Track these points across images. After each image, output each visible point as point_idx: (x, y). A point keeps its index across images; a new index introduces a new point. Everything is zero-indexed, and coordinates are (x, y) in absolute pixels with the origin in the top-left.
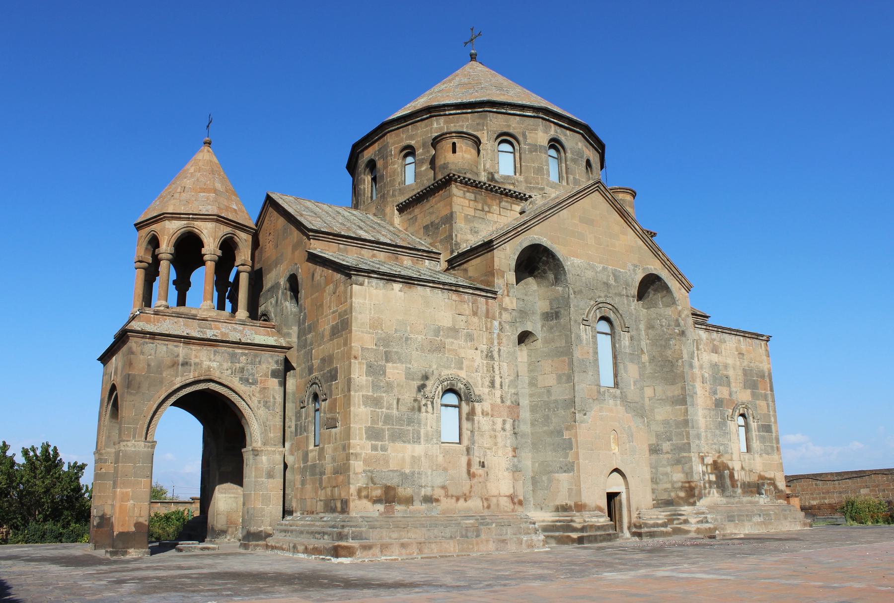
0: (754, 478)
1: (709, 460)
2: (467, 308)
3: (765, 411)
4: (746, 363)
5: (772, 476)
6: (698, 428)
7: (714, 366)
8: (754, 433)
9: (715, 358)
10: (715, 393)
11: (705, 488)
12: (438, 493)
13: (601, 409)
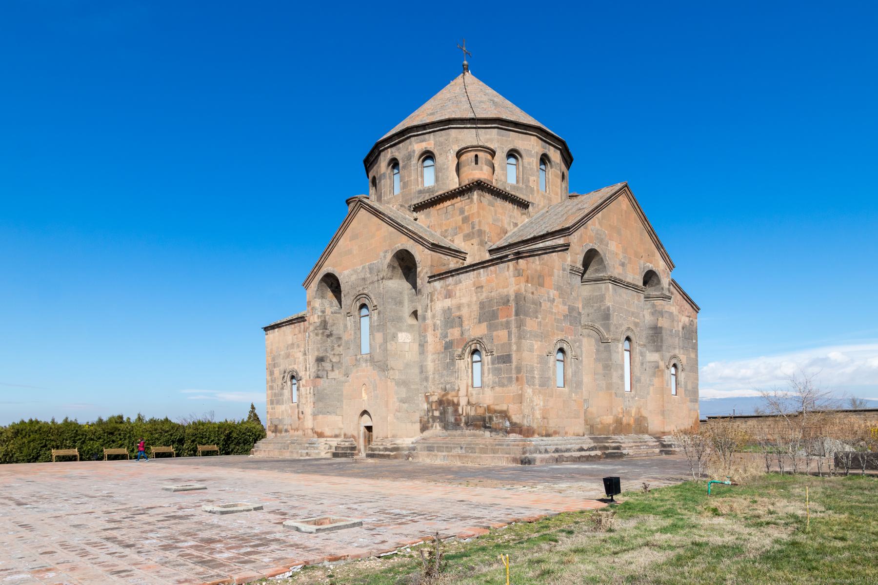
0: (480, 411)
1: (435, 398)
2: (297, 330)
3: (505, 340)
4: (484, 296)
5: (504, 408)
6: (427, 372)
7: (447, 311)
8: (486, 368)
9: (448, 303)
10: (446, 336)
11: (428, 422)
12: (289, 427)
13: (357, 372)
